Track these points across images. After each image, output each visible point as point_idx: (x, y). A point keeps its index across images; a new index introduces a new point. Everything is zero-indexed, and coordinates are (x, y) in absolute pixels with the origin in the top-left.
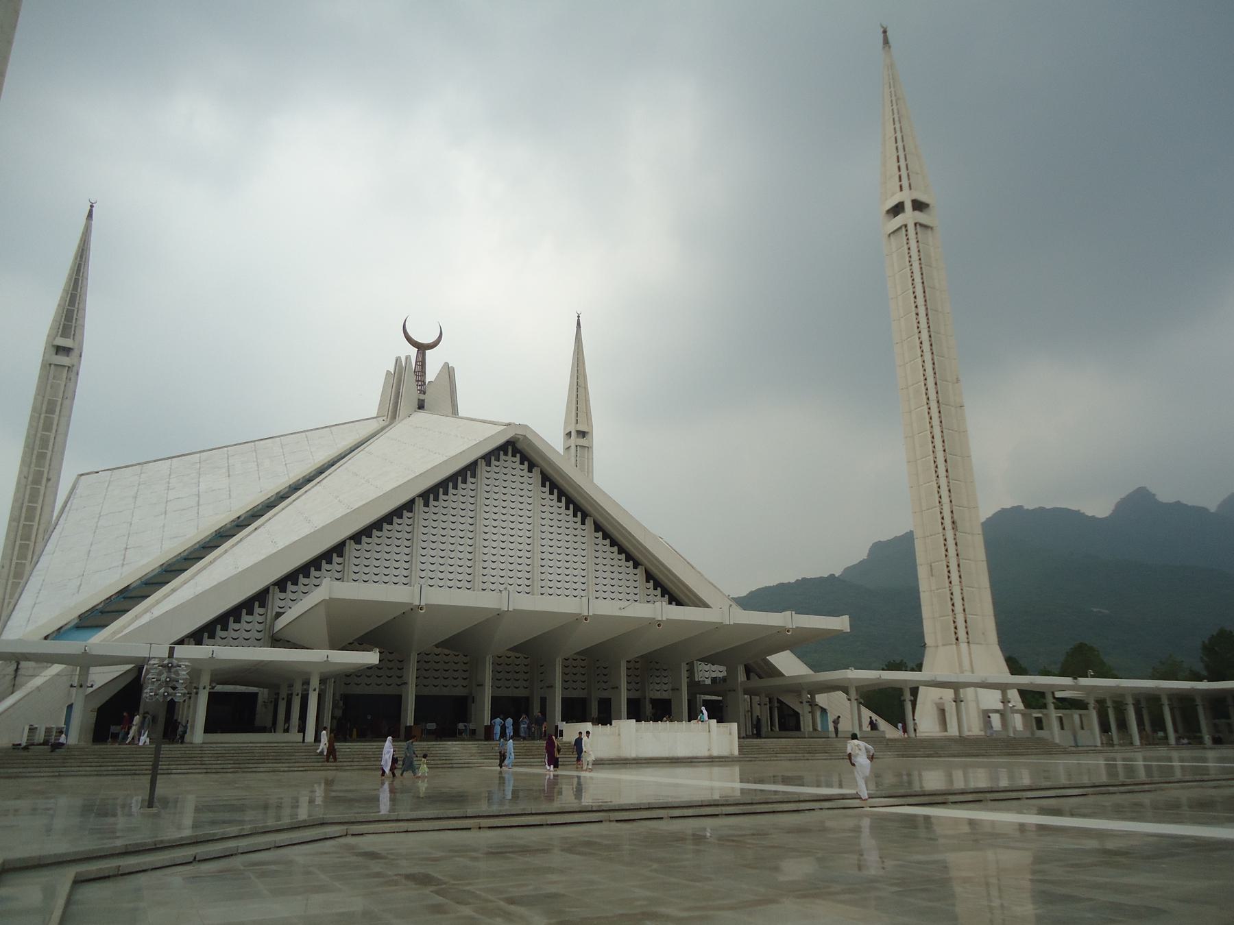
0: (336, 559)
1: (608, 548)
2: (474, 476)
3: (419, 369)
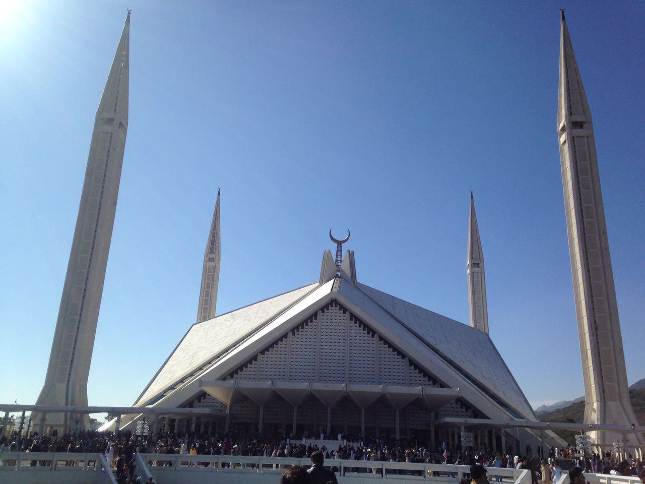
0: (254, 362)
2: (316, 318)
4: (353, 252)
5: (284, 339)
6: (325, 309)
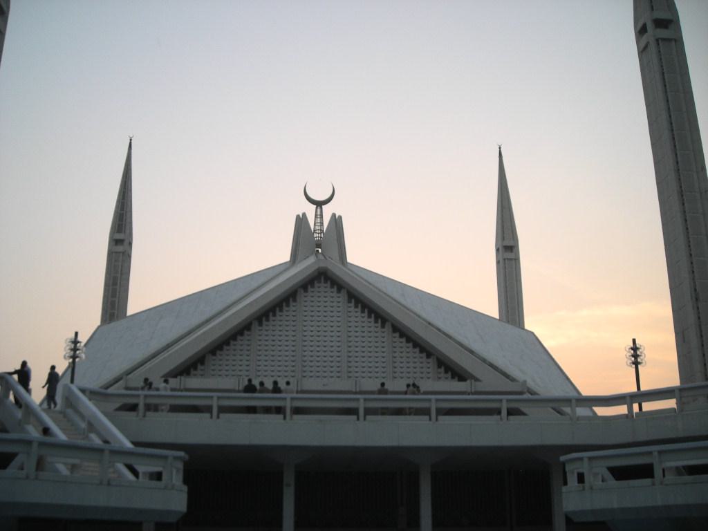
0: (199, 367)
1: (404, 344)
2: (295, 301)
3: (318, 220)
4: (340, 217)
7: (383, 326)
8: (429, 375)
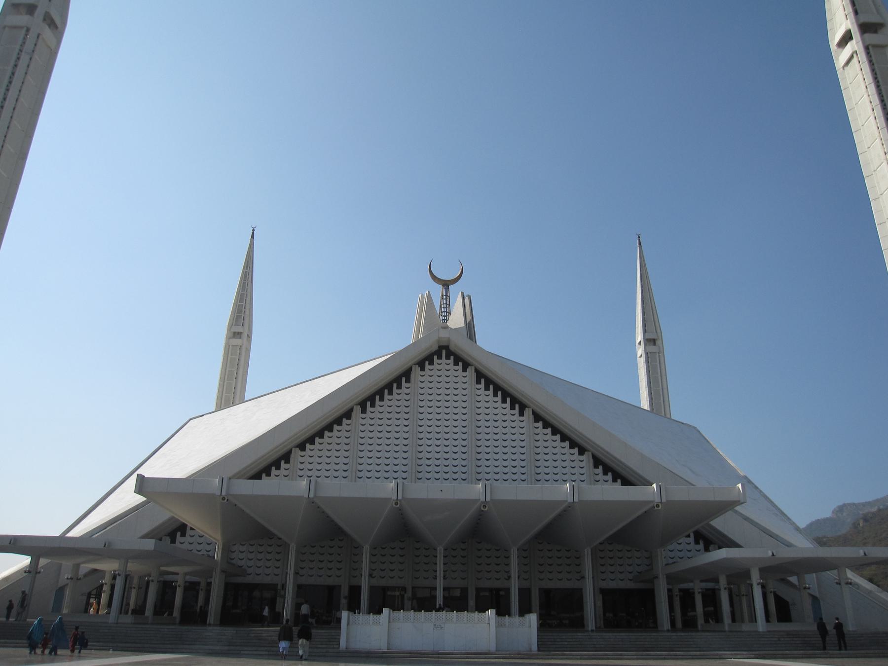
0: (283, 465)
1: (550, 437)
2: (408, 381)
5: (344, 420)
6: (427, 363)
7: (521, 414)
8: (583, 478)
